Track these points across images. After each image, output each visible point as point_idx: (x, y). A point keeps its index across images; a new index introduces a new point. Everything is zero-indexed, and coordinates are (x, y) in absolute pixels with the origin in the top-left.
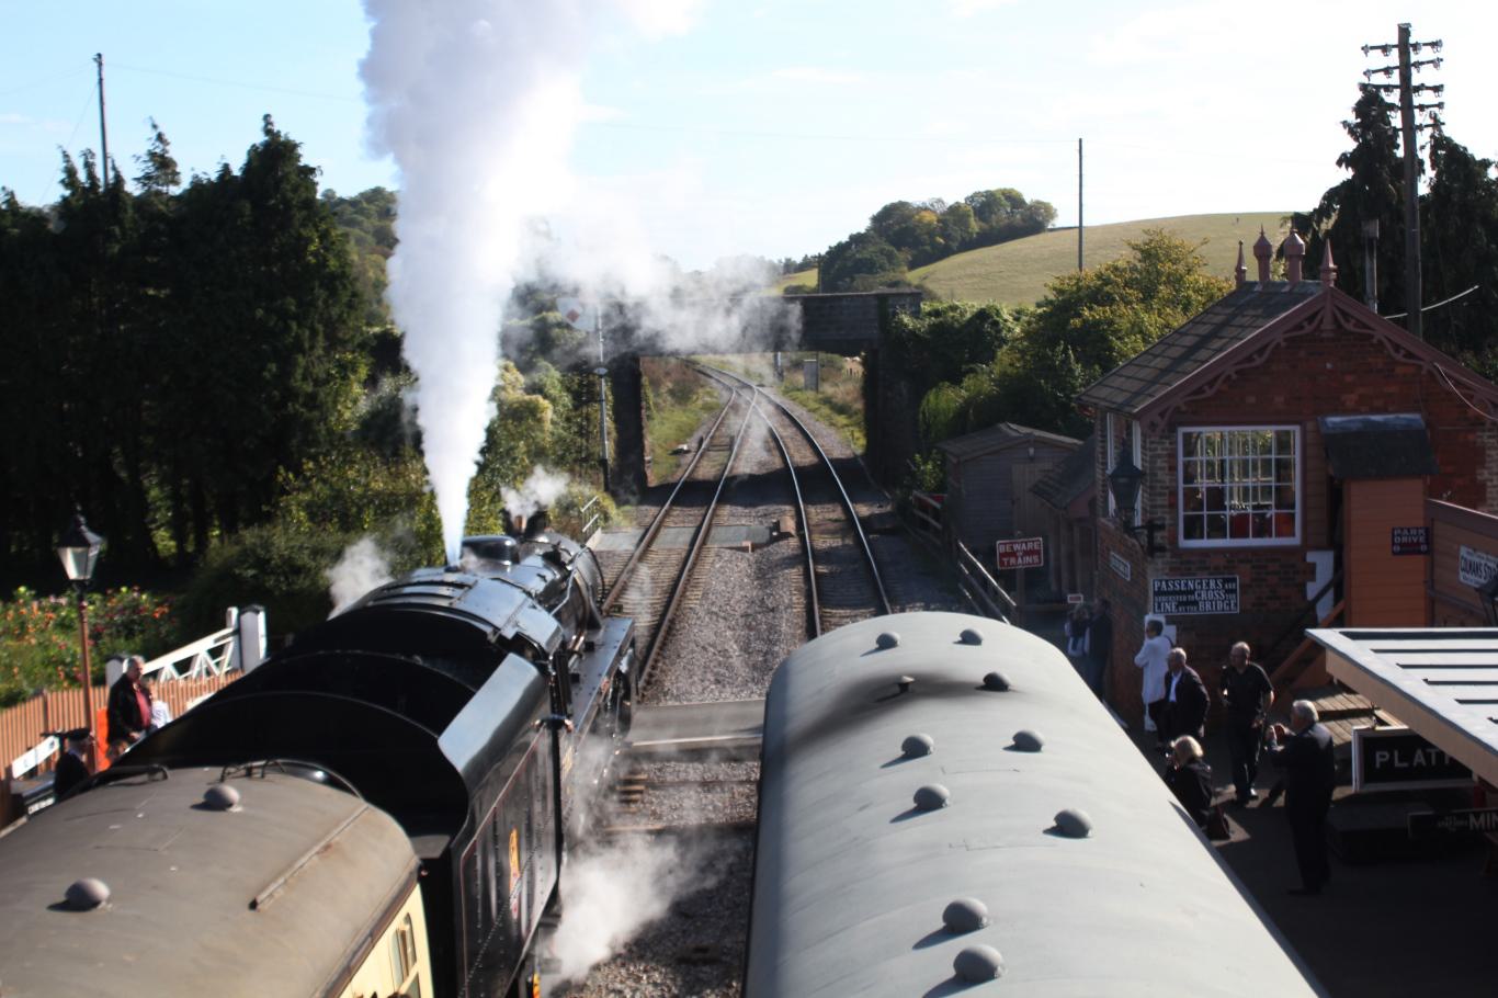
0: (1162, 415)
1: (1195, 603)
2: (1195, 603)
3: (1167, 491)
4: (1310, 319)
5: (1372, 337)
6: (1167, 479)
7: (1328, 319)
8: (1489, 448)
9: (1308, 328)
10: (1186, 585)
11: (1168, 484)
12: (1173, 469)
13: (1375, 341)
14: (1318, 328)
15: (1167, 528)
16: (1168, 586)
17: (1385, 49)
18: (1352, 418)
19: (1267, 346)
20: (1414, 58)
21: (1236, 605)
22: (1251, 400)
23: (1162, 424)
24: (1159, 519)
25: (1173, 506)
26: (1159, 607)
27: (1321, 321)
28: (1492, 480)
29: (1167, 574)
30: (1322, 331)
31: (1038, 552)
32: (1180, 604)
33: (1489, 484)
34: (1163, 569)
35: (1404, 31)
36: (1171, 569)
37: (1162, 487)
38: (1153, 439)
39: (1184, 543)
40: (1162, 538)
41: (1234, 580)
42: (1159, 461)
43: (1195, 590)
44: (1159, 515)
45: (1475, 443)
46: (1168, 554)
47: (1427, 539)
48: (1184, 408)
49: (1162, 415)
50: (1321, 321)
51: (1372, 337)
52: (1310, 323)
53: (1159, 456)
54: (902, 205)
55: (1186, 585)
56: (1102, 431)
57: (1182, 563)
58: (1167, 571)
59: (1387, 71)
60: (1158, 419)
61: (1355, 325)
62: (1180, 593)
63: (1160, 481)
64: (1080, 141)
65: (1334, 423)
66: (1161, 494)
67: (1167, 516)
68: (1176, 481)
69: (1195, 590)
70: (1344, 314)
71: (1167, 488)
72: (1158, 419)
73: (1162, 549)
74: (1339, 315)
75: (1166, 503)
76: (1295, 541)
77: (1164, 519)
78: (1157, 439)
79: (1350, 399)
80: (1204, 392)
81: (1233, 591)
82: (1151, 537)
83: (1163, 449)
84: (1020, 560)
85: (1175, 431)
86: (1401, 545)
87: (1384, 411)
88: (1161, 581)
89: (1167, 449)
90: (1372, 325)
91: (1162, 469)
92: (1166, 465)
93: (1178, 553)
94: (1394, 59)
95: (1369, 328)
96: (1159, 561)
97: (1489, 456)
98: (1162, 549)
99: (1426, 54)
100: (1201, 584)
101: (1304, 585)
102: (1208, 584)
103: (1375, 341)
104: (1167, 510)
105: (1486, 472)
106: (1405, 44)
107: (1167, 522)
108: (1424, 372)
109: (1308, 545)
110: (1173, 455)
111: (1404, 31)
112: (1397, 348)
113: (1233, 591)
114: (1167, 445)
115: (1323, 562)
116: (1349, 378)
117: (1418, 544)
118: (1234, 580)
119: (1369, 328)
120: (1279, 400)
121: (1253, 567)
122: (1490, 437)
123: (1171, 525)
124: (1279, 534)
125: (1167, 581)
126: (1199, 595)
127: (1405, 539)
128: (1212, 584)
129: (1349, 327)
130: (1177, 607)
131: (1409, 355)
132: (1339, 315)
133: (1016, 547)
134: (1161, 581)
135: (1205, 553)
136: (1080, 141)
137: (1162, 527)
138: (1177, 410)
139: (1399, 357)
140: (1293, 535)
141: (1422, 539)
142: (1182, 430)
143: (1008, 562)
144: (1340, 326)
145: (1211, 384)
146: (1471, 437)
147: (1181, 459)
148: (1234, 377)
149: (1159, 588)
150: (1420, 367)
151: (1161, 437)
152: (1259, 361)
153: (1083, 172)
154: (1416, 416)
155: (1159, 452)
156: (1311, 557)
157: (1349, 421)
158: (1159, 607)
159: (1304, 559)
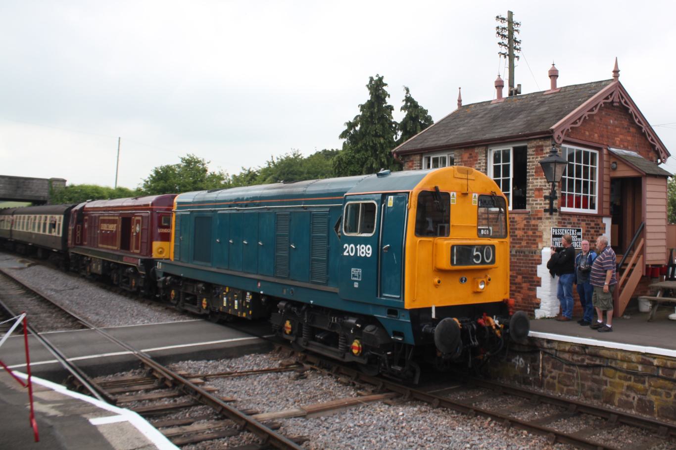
4: (611, 95)
27: (614, 98)
29: (557, 225)
34: (556, 222)
35: (511, 14)
36: (559, 223)
58: (557, 223)
76: (595, 212)
93: (562, 214)
94: (506, 25)
95: (628, 105)
100: (569, 232)
102: (572, 232)
106: (510, 22)
111: (511, 14)
119: (628, 105)
159: (602, 222)
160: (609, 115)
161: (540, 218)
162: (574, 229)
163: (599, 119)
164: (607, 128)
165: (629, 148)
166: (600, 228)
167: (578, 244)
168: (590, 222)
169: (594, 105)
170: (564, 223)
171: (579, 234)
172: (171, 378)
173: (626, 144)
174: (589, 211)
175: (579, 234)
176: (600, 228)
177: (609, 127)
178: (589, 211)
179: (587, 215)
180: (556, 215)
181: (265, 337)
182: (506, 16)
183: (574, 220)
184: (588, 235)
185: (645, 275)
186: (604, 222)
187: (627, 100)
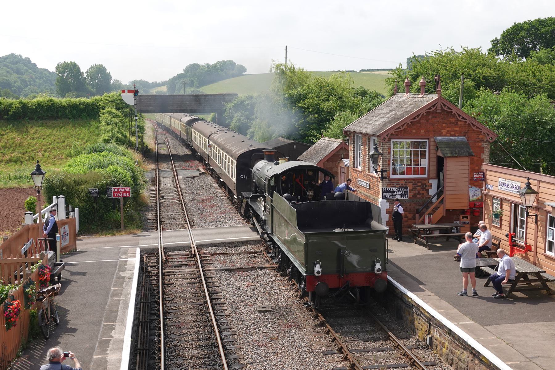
0: (387, 135)
1: (395, 195)
2: (395, 195)
3: (387, 160)
5: (452, 112)
6: (388, 156)
7: (439, 106)
8: (485, 148)
9: (433, 109)
10: (393, 190)
11: (388, 158)
12: (389, 153)
13: (453, 113)
16: (387, 190)
18: (445, 138)
19: (420, 114)
21: (407, 196)
22: (414, 131)
23: (387, 138)
24: (384, 169)
25: (389, 165)
26: (384, 197)
27: (437, 107)
28: (485, 158)
30: (437, 110)
32: (390, 196)
36: (388, 185)
37: (386, 159)
38: (383, 143)
39: (392, 177)
41: (407, 188)
42: (385, 150)
43: (395, 191)
45: (481, 146)
46: (387, 180)
48: (394, 133)
49: (387, 135)
50: (437, 107)
51: (452, 112)
53: (385, 148)
55: (393, 190)
56: (353, 140)
57: (391, 183)
60: (386, 137)
61: (447, 108)
62: (391, 192)
63: (385, 157)
64: (286, 46)
65: (439, 139)
66: (386, 161)
67: (387, 168)
68: (390, 156)
69: (395, 191)
71: (387, 159)
72: (386, 137)
73: (385, 178)
75: (387, 164)
76: (426, 176)
77: (386, 169)
78: (385, 143)
79: (444, 132)
80: (400, 128)
81: (407, 192)
82: (382, 175)
83: (386, 146)
85: (390, 141)
86: (476, 177)
87: (454, 135)
88: (385, 188)
89: (388, 146)
93: (390, 180)
96: (384, 182)
97: (485, 150)
98: (385, 178)
100: (397, 189)
101: (428, 190)
102: (399, 190)
103: (453, 113)
105: (484, 155)
107: (387, 170)
108: (467, 124)
110: (389, 148)
112: (459, 116)
113: (407, 192)
114: (388, 145)
115: (434, 183)
116: (444, 125)
117: (481, 177)
118: (407, 188)
120: (423, 131)
121: (413, 184)
122: (485, 144)
123: (388, 171)
125: (387, 188)
126: (396, 193)
127: (477, 176)
128: (401, 189)
129: (445, 109)
130: (389, 197)
131: (463, 118)
134: (385, 188)
135: (399, 180)
136: (286, 46)
137: (386, 171)
138: (392, 134)
139: (460, 119)
140: (425, 174)
142: (392, 141)
144: (442, 108)
145: (403, 126)
146: (480, 144)
148: (410, 124)
149: (384, 191)
150: (466, 122)
151: (386, 143)
152: (417, 119)
153: (287, 57)
154: (464, 137)
155: (385, 147)
156: (431, 181)
157: (444, 139)
158: (384, 197)
159: (429, 182)
160: (436, 117)
162: (402, 188)
163: (425, 121)
165: (456, 135)
166: (426, 186)
167: (405, 196)
169: (418, 114)
170: (394, 185)
171: (406, 190)
172: (193, 253)
173: (453, 133)
175: (406, 190)
176: (426, 186)
180: (385, 181)
181: (423, 236)
183: (403, 182)
184: (414, 190)
185: (445, 215)
186: (430, 182)
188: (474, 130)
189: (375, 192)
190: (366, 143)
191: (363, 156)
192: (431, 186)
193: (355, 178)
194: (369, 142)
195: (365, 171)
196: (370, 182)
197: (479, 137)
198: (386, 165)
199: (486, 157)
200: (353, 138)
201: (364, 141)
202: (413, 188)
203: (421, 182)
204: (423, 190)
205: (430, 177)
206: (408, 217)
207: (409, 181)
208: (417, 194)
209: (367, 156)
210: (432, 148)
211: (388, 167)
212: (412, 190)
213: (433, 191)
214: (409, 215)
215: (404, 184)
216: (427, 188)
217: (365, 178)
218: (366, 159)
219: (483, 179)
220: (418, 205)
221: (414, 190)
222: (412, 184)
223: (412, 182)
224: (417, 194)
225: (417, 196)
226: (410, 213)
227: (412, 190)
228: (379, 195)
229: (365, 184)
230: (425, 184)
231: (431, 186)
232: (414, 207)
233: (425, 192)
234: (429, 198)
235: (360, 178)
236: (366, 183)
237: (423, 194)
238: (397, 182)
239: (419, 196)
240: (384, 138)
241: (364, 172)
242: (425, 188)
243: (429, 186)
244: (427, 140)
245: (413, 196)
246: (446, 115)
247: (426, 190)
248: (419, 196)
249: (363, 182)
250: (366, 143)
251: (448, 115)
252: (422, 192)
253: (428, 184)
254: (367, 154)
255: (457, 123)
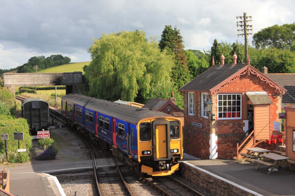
5: (257, 75)
6: (215, 105)
9: (245, 73)
12: (217, 103)
13: (257, 76)
14: (246, 74)
15: (215, 115)
17: (241, 17)
20: (246, 20)
25: (217, 110)
31: (48, 134)
33: (279, 106)
40: (214, 117)
42: (214, 101)
44: (214, 113)
47: (285, 115)
51: (257, 75)
52: (245, 72)
54: (35, 57)
57: (218, 123)
59: (241, 22)
60: (215, 92)
66: (214, 108)
67: (215, 113)
70: (252, 71)
74: (250, 70)
75: (215, 110)
76: (240, 118)
84: (43, 136)
90: (257, 73)
91: (214, 103)
92: (215, 102)
94: (243, 20)
95: (256, 73)
99: (249, 19)
101: (242, 127)
103: (257, 76)
104: (215, 111)
105: (278, 104)
107: (215, 114)
109: (243, 119)
111: (245, 14)
114: (216, 98)
115: (246, 122)
117: (283, 116)
119: (256, 73)
124: (224, 117)
129: (253, 73)
132: (250, 70)
133: (42, 133)
137: (214, 115)
139: (262, 79)
141: (284, 115)
143: (40, 136)
147: (189, 103)
156: (244, 121)
159: (243, 122)
161: (210, 122)
164: (245, 84)
166: (241, 125)
168: (235, 123)
174: (236, 118)
176: (241, 125)
177: (246, 84)
178: (236, 118)
179: (233, 120)
182: (243, 16)
187: (255, 71)
188: (271, 87)
189: (207, 130)
190: (198, 97)
191: (195, 106)
192: (244, 124)
193: (189, 121)
194: (200, 96)
195: (197, 116)
196: (202, 123)
197: (274, 91)
198: (215, 111)
199: (279, 105)
200: (186, 94)
201: (196, 96)
202: (233, 126)
203: (237, 122)
204: (239, 128)
205: (244, 118)
206: (229, 146)
207: (230, 121)
208: (235, 130)
209: (199, 106)
210: (244, 99)
211: (216, 112)
212: (232, 128)
213: (246, 128)
214: (230, 144)
215: (227, 124)
216: (241, 126)
217: (197, 121)
218: (198, 108)
219: (284, 117)
220: (237, 138)
221: (234, 128)
222: (231, 123)
223: (232, 122)
224: (235, 130)
225: (235, 132)
226: (231, 143)
227: (232, 128)
228: (210, 132)
229: (198, 125)
230: (240, 123)
231: (244, 125)
232: (234, 139)
233: (240, 129)
234: (243, 133)
235: (193, 121)
236: (199, 124)
237: (239, 130)
238: (222, 122)
239: (237, 132)
240: (213, 93)
241: (196, 117)
242: (240, 126)
243: (243, 125)
244: (241, 94)
245: (233, 132)
246: (253, 77)
247: (241, 127)
248: (237, 132)
249: (196, 124)
250: (198, 97)
251: (254, 77)
252: (238, 129)
253: (242, 123)
254: (199, 105)
255: (260, 82)
